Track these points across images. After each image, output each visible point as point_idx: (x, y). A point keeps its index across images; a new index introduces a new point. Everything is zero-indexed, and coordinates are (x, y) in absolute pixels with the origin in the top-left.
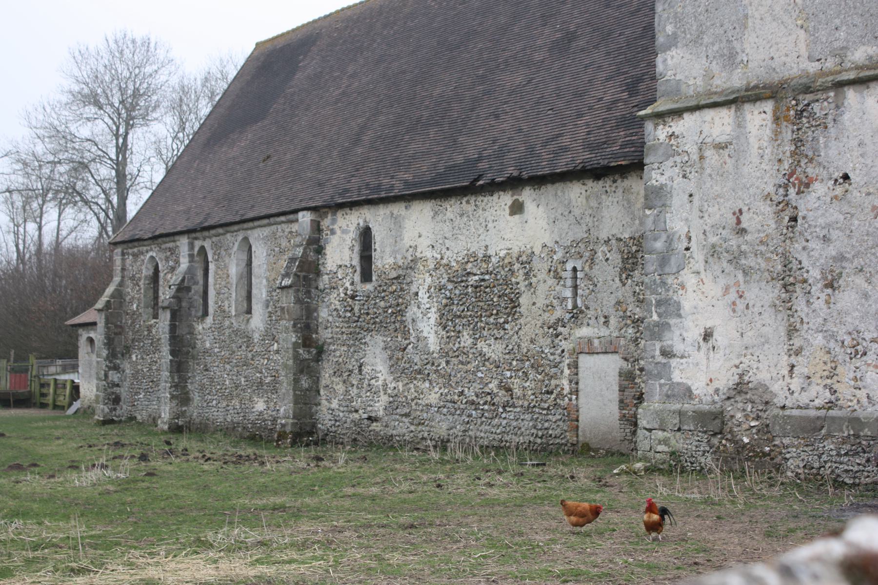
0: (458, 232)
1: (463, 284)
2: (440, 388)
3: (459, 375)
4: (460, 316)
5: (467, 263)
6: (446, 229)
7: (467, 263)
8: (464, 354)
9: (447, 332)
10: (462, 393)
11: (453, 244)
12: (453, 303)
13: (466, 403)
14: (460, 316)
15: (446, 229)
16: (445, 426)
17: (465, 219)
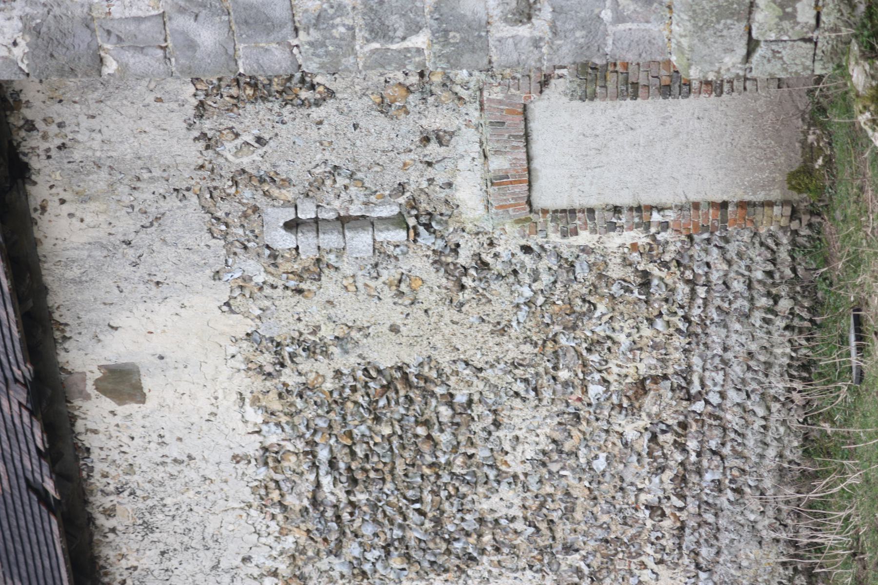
0: (197, 535)
1: (346, 517)
2: (643, 565)
3: (605, 518)
4: (437, 521)
5: (284, 508)
6: (189, 567)
7: (284, 508)
8: (542, 505)
9: (483, 551)
10: (654, 509)
11: (233, 547)
12: (401, 540)
13: (683, 497)
14: (437, 521)
15: (189, 567)
16: (749, 552)
17: (159, 518)
